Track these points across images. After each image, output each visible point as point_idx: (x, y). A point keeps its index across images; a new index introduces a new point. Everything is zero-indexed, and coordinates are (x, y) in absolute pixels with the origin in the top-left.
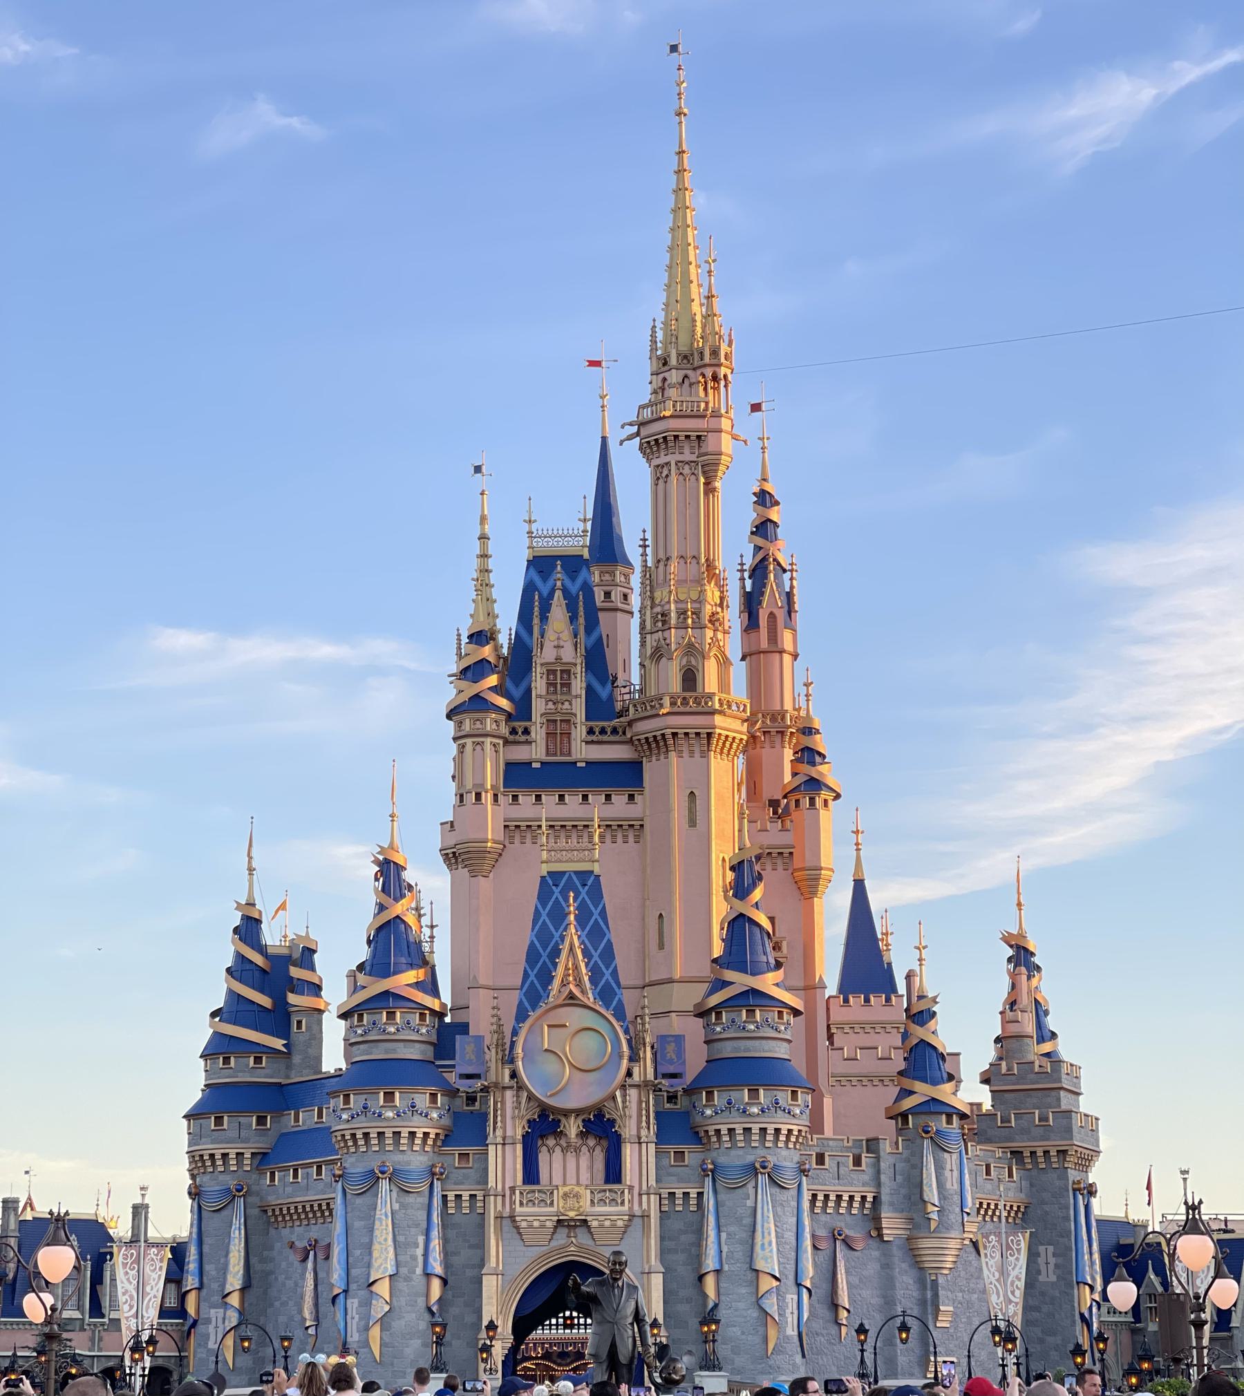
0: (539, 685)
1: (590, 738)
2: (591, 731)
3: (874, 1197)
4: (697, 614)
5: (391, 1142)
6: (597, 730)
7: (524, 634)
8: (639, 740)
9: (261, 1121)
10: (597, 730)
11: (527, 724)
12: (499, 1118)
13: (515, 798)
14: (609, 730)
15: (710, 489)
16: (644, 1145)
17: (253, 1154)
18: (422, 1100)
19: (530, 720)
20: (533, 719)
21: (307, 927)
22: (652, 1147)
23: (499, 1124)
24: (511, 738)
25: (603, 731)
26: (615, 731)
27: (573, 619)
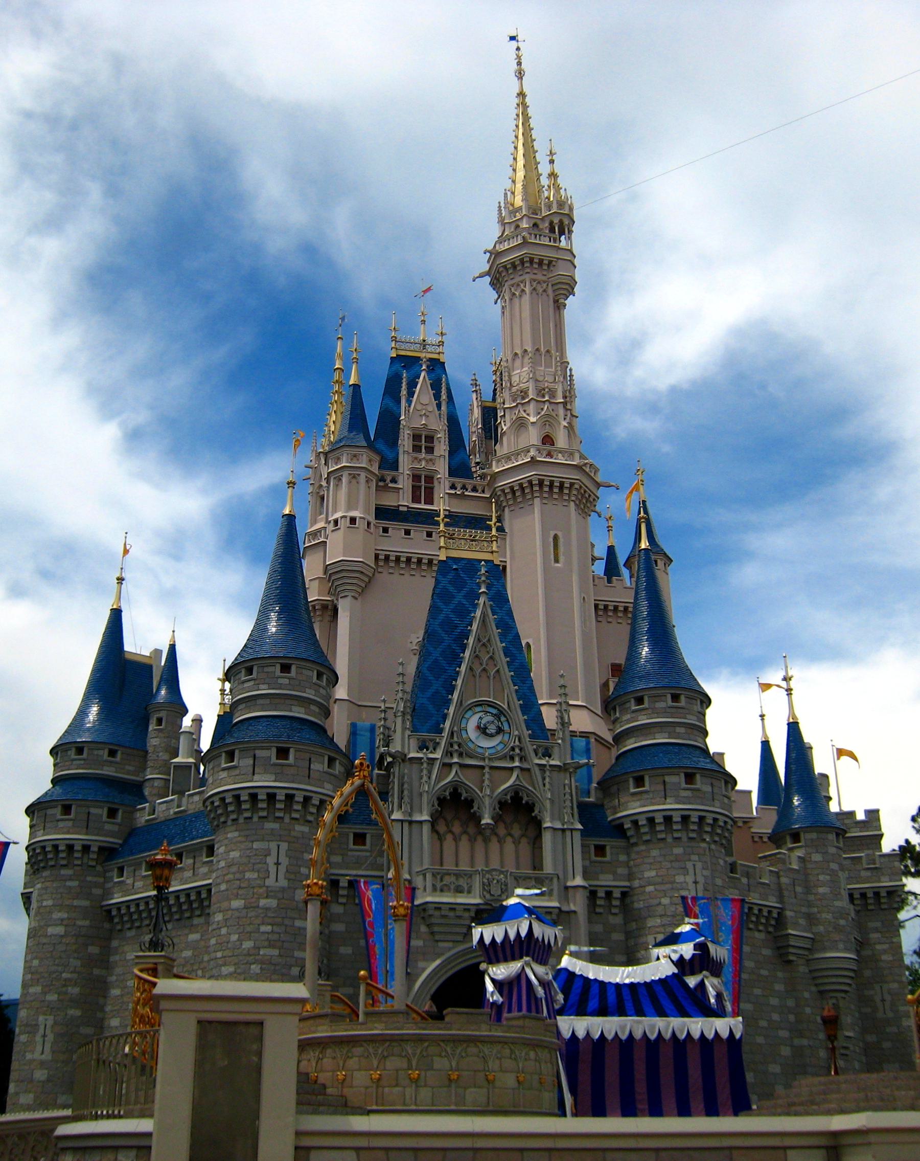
0: (405, 442)
1: (453, 492)
2: (453, 487)
3: (779, 913)
4: (553, 393)
5: (283, 806)
6: (459, 486)
7: (391, 404)
8: (503, 491)
9: (112, 813)
10: (459, 486)
11: (394, 473)
12: (406, 793)
13: (385, 530)
14: (470, 487)
15: (559, 306)
16: (568, 833)
17: (101, 849)
18: (319, 766)
19: (397, 469)
20: (401, 470)
21: (174, 631)
22: (577, 836)
23: (406, 799)
24: (381, 484)
25: (464, 487)
26: (474, 489)
27: (437, 396)
